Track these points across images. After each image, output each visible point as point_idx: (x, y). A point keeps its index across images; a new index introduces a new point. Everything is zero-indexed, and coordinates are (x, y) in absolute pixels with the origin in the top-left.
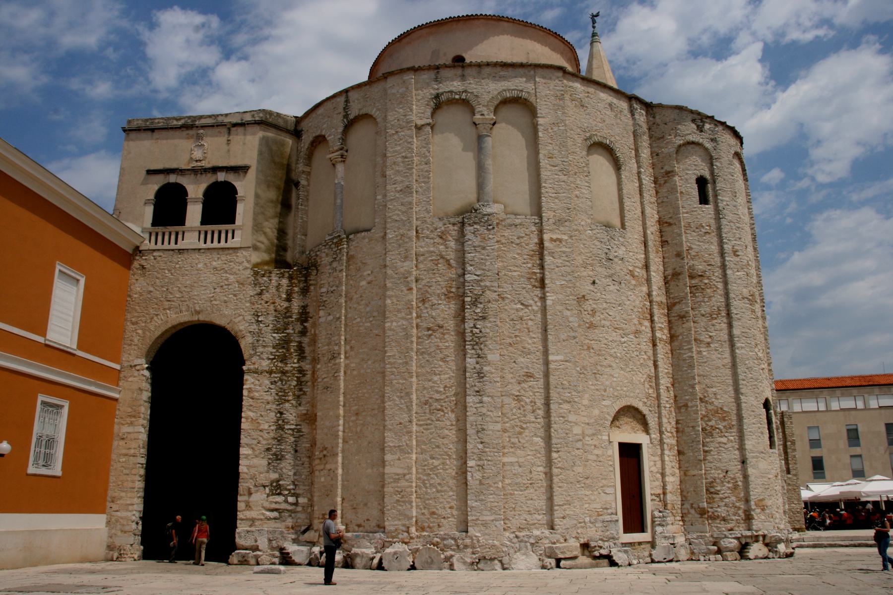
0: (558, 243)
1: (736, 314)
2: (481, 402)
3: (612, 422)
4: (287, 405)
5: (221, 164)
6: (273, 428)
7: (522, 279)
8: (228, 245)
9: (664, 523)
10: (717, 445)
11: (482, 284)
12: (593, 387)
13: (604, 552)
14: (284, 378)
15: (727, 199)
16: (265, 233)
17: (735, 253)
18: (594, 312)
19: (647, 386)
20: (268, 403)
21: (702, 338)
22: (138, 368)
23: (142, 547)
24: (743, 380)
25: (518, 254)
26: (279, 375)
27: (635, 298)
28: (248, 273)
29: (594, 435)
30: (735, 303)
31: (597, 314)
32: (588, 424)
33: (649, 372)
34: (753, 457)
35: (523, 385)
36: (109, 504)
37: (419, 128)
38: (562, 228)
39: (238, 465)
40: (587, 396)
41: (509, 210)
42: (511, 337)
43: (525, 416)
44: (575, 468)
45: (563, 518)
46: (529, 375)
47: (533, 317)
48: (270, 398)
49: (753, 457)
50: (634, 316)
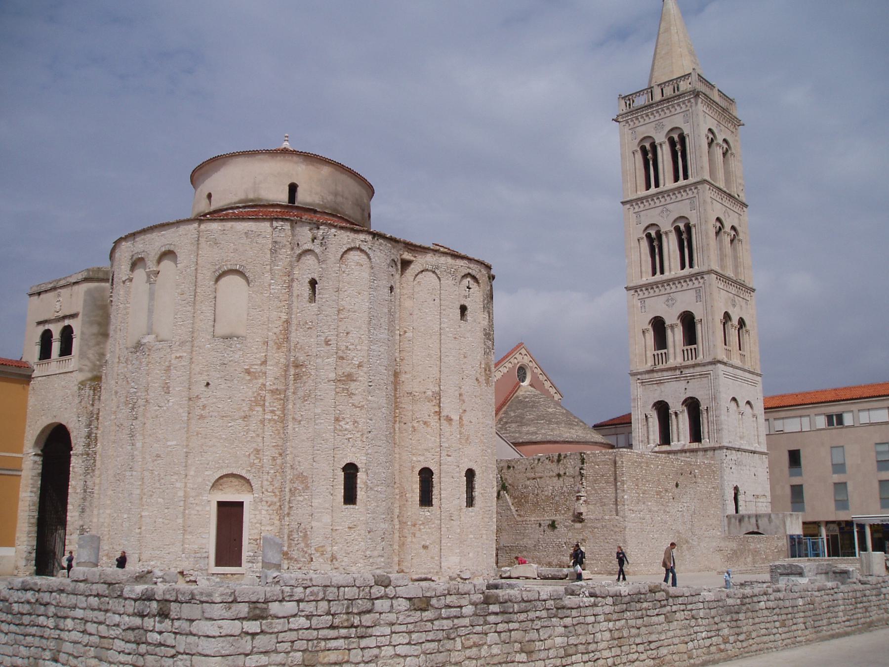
0: (180, 359)
1: (320, 395)
3: (211, 487)
5: (68, 313)
6: (82, 491)
7: (160, 388)
9: (254, 561)
10: (297, 503)
11: (137, 394)
12: (199, 462)
13: (192, 578)
14: (88, 458)
15: (327, 296)
16: (88, 358)
17: (327, 343)
18: (204, 407)
19: (252, 457)
20: (80, 476)
21: (296, 417)
22: (30, 455)
23: (35, 568)
24: (318, 450)
25: (159, 370)
26: (85, 456)
27: (247, 391)
28: (76, 388)
29: (196, 496)
30: (320, 386)
31: (207, 408)
32: (193, 489)
33: (256, 447)
34: (318, 512)
36: (16, 542)
37: (124, 282)
39: (66, 516)
40: (194, 468)
41: (159, 339)
42: (151, 430)
43: (154, 484)
44: (178, 520)
45: (169, 553)
46: (158, 456)
47: (163, 415)
48: (81, 472)
49: (318, 512)
50: (244, 405)
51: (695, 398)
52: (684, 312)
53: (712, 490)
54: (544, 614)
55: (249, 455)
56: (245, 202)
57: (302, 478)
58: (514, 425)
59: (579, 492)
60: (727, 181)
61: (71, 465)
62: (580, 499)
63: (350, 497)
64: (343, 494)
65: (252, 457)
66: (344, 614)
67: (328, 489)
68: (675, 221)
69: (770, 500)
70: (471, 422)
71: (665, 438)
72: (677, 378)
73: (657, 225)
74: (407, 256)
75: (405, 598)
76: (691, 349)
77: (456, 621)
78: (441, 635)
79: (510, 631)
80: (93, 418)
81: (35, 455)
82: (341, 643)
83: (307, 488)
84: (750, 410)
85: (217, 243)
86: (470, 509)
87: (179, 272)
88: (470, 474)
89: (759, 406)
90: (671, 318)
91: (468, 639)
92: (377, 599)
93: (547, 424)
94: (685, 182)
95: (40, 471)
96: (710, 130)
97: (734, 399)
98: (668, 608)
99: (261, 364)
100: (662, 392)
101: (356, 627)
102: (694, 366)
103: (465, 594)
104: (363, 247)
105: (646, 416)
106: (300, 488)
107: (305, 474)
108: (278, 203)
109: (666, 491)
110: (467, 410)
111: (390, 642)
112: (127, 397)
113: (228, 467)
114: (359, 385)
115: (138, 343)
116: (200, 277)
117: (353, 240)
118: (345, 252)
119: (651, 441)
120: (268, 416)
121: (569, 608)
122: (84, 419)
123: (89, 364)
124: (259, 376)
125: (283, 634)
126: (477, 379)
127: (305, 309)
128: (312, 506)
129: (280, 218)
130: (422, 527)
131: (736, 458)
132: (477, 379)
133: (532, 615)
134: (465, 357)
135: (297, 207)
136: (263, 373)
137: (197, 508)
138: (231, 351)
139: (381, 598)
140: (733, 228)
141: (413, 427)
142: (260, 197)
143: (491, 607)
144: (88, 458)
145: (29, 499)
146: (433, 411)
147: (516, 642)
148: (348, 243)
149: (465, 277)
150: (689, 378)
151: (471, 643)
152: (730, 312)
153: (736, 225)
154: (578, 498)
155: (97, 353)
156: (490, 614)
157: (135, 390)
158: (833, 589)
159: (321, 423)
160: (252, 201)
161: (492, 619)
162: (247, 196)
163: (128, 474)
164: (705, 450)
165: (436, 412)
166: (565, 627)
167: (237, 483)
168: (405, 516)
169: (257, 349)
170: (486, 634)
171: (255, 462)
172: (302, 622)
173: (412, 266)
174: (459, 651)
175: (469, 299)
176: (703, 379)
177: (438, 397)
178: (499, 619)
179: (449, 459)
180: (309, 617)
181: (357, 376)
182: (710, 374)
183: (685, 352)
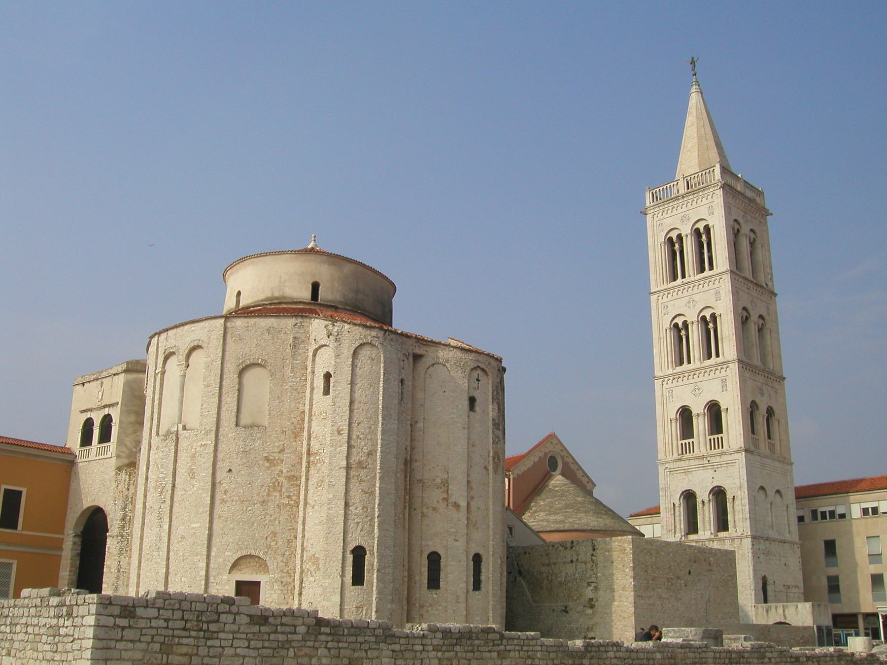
2: (159, 555)
4: (123, 556)
6: (116, 571)
8: (106, 456)
12: (219, 544)
14: (122, 540)
15: (340, 388)
16: (125, 446)
17: (339, 433)
18: (226, 492)
22: (70, 536)
24: (329, 534)
28: (114, 473)
31: (229, 493)
34: (329, 592)
35: (180, 544)
38: (208, 437)
51: (722, 487)
52: (711, 401)
53: (729, 578)
54: (373, 639)
55: (267, 537)
56: (271, 300)
57: (315, 560)
58: (542, 514)
59: (590, 577)
60: (754, 272)
61: (107, 546)
62: (591, 586)
63: (358, 579)
64: (351, 575)
65: (269, 539)
66: (195, 621)
67: (337, 570)
68: (701, 311)
69: (802, 591)
70: (478, 508)
71: (692, 527)
72: (704, 467)
73: (684, 315)
74: (418, 351)
75: (246, 615)
76: (718, 438)
77: (289, 636)
78: (275, 645)
79: (339, 648)
80: (128, 502)
81: (75, 536)
82: (190, 641)
83: (319, 569)
84: (781, 499)
85: (240, 339)
86: (477, 592)
87: (206, 365)
88: (477, 559)
89: (790, 496)
90: (698, 408)
91: (301, 650)
92: (223, 613)
93: (576, 513)
94: (711, 273)
95: (79, 552)
96: (735, 221)
97: (762, 488)
98: (502, 647)
99: (280, 452)
100: (689, 481)
101: (205, 631)
102: (720, 455)
103: (300, 617)
104: (373, 343)
105: (674, 505)
106: (312, 569)
107: (317, 556)
108: (302, 300)
109: (678, 578)
110: (475, 496)
111: (232, 645)
112: (157, 482)
113: (247, 548)
114: (368, 473)
115: (167, 432)
116: (226, 370)
117: (365, 337)
118: (358, 347)
119: (678, 530)
120: (286, 501)
121: (398, 637)
122: (120, 503)
123: (126, 450)
124: (277, 464)
125: (146, 630)
126: (485, 468)
127: (321, 402)
128: (322, 586)
129: (300, 316)
130: (429, 609)
131: (764, 548)
132: (485, 468)
133: (360, 639)
134: (473, 446)
135: (320, 305)
136: (281, 460)
137: (218, 587)
138: (252, 439)
139: (227, 613)
140: (761, 317)
141: (422, 513)
142: (285, 295)
143: (323, 629)
144: (122, 540)
145: (67, 577)
146: (442, 497)
147: (345, 657)
148: (361, 339)
149: (474, 371)
150: (715, 467)
151: (302, 653)
152: (758, 402)
153: (764, 314)
154: (589, 584)
155: (134, 441)
156: (320, 634)
157: (165, 476)
158: (701, 648)
159: (332, 508)
160: (277, 298)
161: (322, 638)
162: (273, 293)
163: (155, 553)
164: (733, 540)
165: (444, 499)
166: (393, 651)
167: (255, 563)
168: (414, 599)
169: (276, 438)
170: (317, 649)
171: (273, 544)
172: (162, 623)
173: (424, 360)
174: (291, 658)
175: (477, 391)
176: (730, 468)
177: (445, 484)
178: (330, 638)
179: (456, 544)
180: (167, 620)
181: (367, 463)
182: (735, 462)
183: (712, 441)
